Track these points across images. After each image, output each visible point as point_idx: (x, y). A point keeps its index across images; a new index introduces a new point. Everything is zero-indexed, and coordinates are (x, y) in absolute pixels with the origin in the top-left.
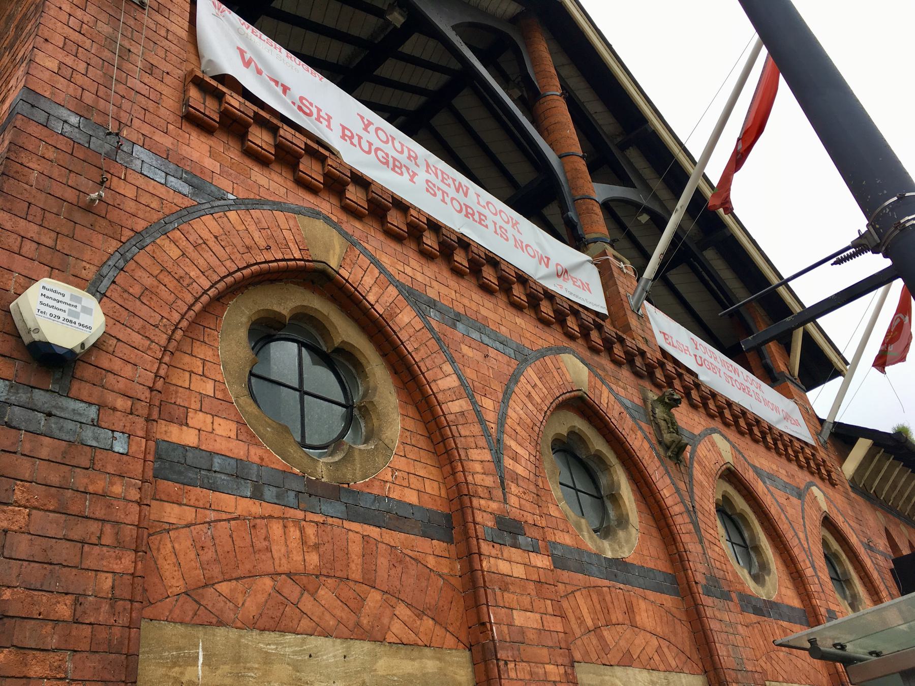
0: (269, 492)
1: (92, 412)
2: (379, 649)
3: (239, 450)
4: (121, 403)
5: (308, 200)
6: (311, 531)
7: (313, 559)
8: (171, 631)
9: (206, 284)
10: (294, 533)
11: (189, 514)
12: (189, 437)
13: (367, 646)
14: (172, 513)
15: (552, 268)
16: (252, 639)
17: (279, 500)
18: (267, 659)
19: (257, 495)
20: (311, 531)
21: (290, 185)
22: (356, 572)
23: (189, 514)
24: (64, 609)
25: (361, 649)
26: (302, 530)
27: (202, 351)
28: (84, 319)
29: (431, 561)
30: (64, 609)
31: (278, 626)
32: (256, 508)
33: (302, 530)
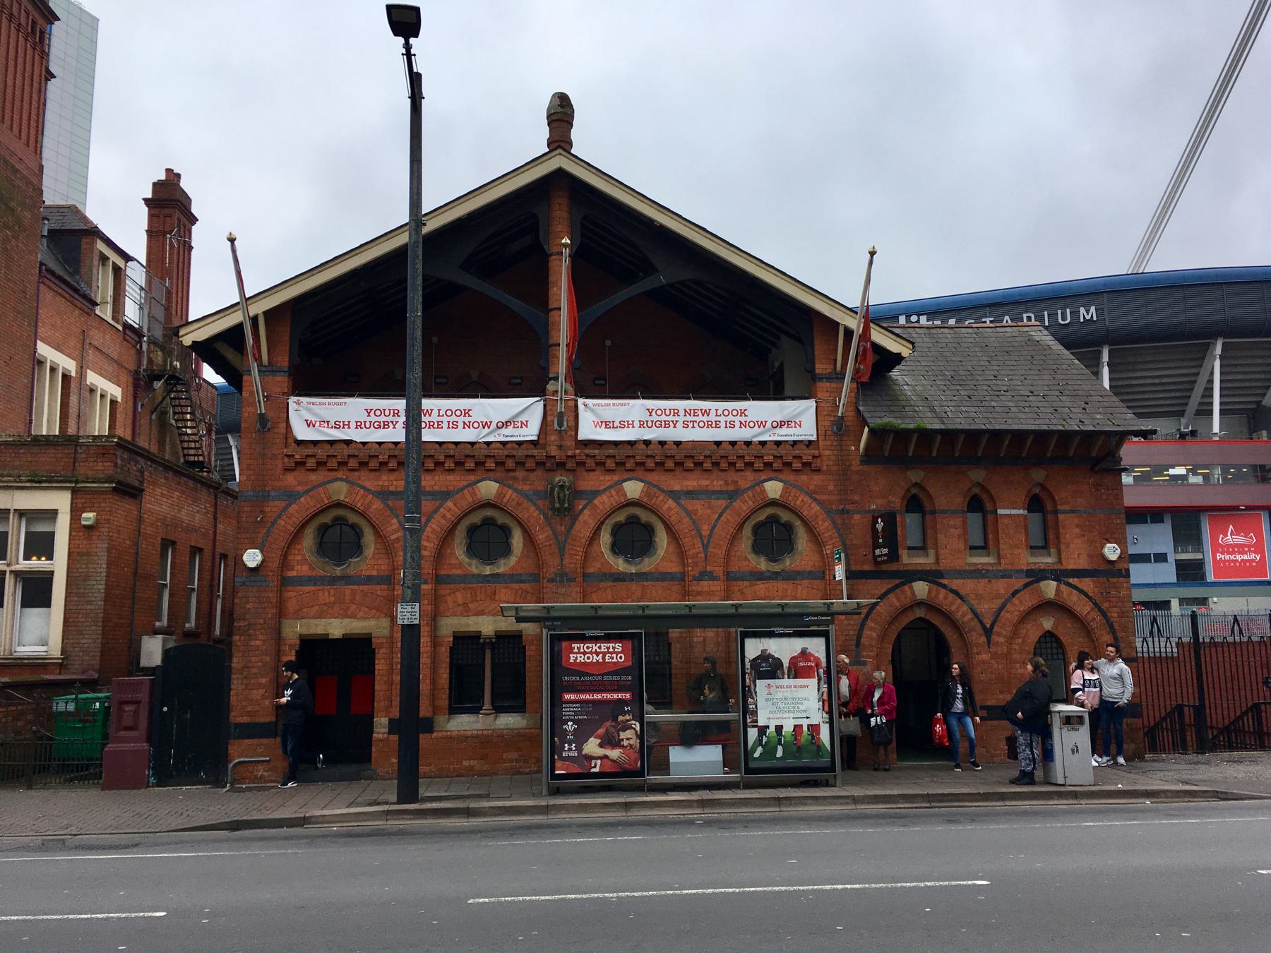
0: (319, 583)
1: (264, 578)
2: (353, 620)
3: (309, 573)
4: (271, 574)
5: (333, 474)
6: (332, 591)
7: (332, 599)
8: (290, 621)
9: (293, 529)
10: (326, 594)
11: (295, 594)
12: (295, 573)
13: (349, 620)
14: (290, 594)
15: (493, 426)
16: (312, 621)
17: (322, 585)
18: (316, 625)
19: (315, 584)
20: (332, 591)
21: (326, 472)
22: (347, 598)
23: (295, 594)
24: (262, 622)
25: (346, 621)
26: (329, 592)
27: (298, 547)
28: (257, 558)
29: (379, 592)
30: (262, 622)
31: (320, 617)
32: (314, 588)
33: (329, 592)
